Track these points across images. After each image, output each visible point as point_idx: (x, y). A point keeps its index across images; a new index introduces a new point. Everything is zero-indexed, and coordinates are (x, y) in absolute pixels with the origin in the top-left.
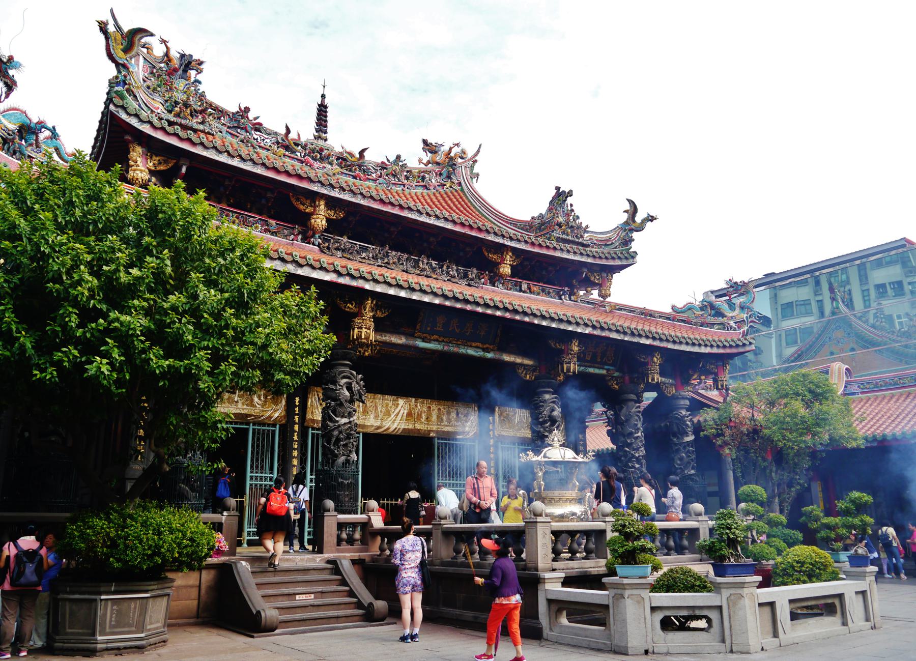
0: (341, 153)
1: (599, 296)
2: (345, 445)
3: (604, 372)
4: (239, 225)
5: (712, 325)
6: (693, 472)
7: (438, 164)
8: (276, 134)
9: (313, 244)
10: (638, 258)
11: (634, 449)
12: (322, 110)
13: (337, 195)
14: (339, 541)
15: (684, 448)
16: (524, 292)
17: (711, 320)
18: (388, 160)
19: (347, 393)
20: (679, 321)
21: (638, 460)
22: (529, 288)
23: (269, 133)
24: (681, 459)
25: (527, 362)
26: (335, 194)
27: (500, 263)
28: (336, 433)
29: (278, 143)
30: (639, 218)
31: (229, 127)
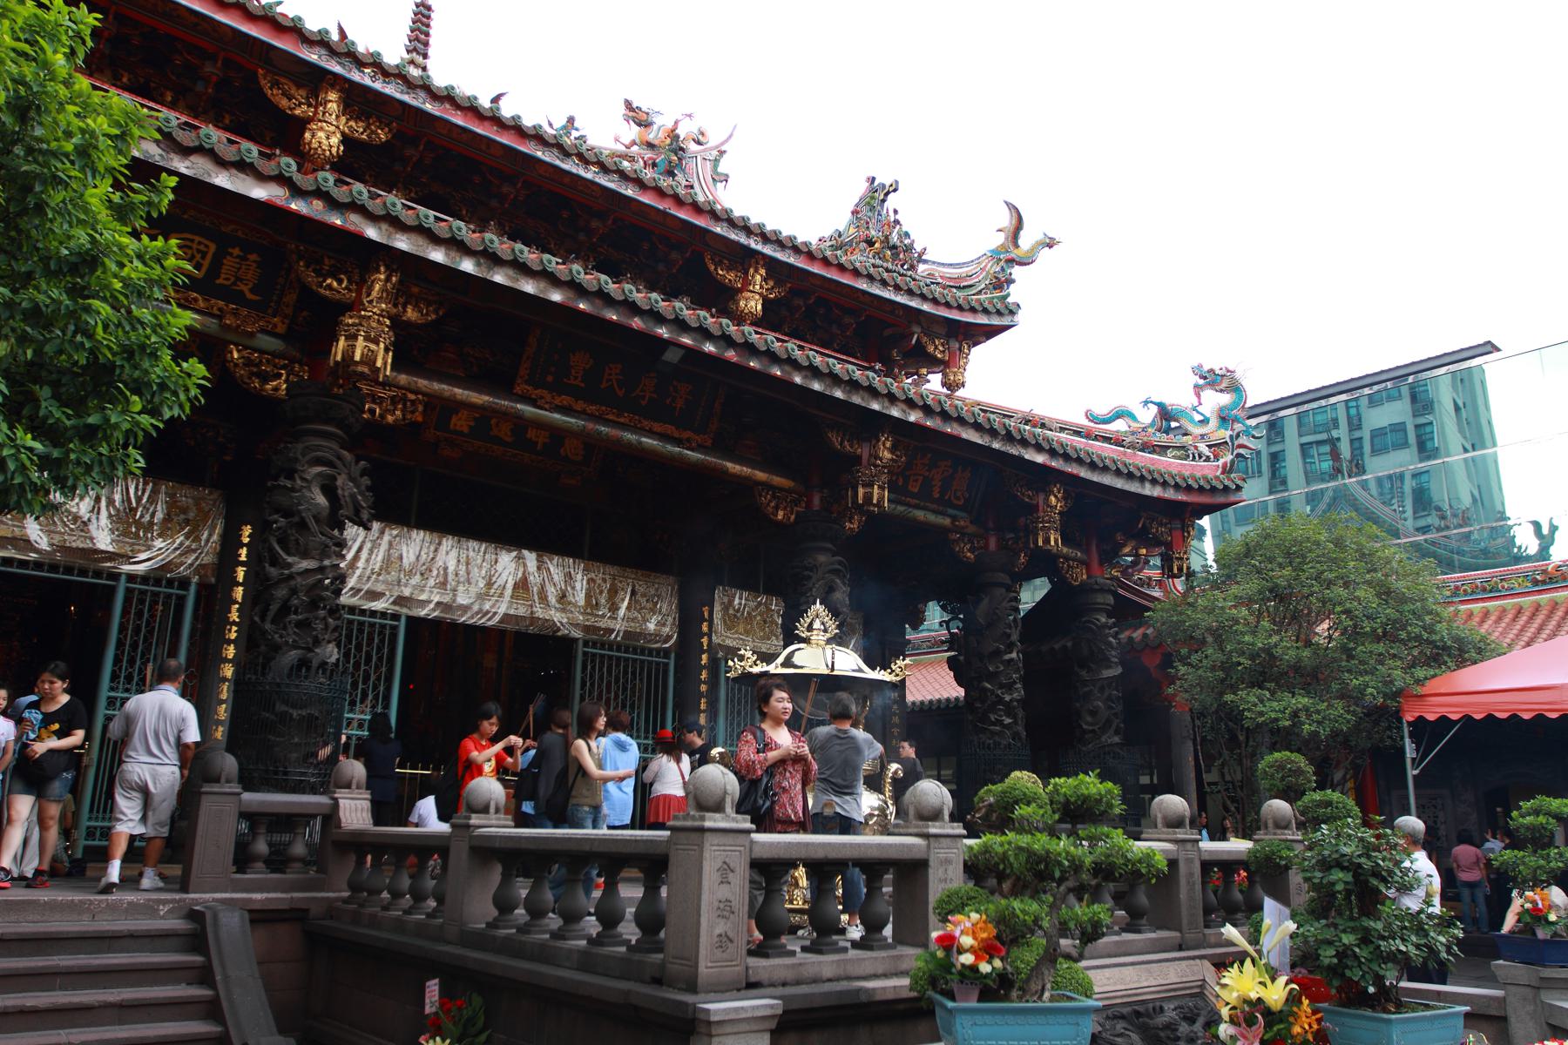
1: (944, 384)
2: (304, 625)
3: (947, 521)
5: (1162, 449)
6: (1117, 739)
7: (650, 146)
10: (1020, 317)
11: (1001, 686)
13: (368, 82)
14: (243, 858)
15: (1102, 689)
17: (1162, 439)
18: (551, 125)
19: (321, 500)
20: (1096, 438)
21: (1009, 710)
24: (1093, 713)
25: (777, 480)
26: (364, 78)
27: (740, 291)
28: (281, 592)
30: (1026, 241)
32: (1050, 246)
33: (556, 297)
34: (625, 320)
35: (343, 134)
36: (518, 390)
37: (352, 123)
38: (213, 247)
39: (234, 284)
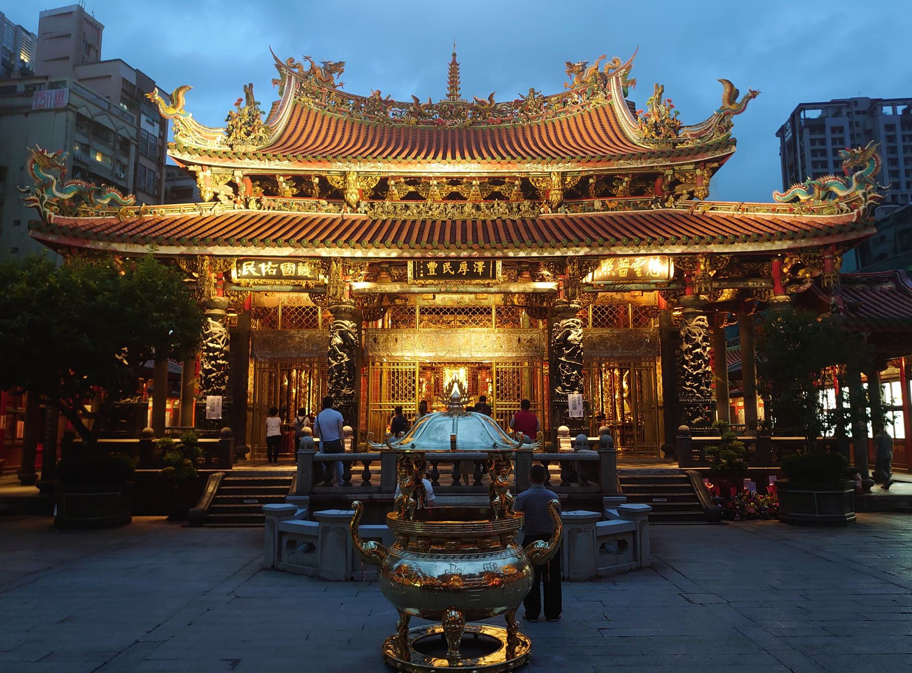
0: (472, 104)
4: (299, 210)
8: (407, 105)
12: (454, 67)
16: (598, 211)
22: (603, 204)
23: (402, 105)
29: (411, 112)
31: (369, 113)
32: (754, 97)
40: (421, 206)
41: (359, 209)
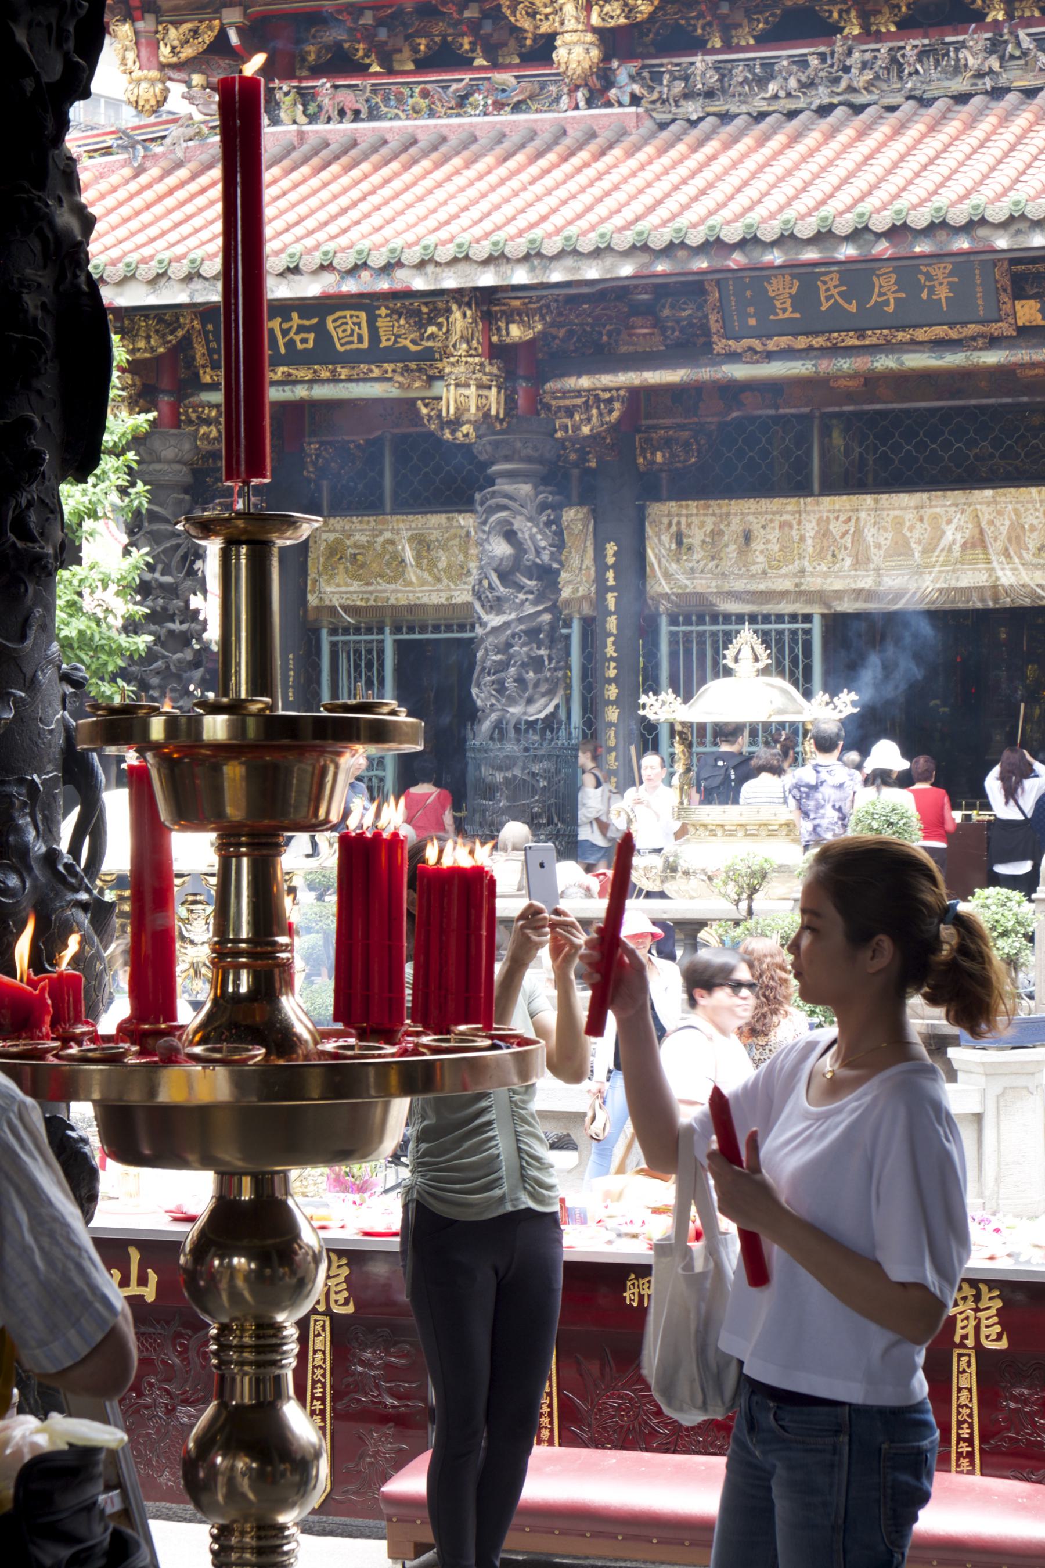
4: (432, 114)
9: (621, 104)
33: (626, 270)
34: (718, 264)
35: (595, 30)
36: (720, 346)
37: (607, 8)
38: (363, 316)
39: (396, 342)
40: (814, 62)
41: (613, 93)
